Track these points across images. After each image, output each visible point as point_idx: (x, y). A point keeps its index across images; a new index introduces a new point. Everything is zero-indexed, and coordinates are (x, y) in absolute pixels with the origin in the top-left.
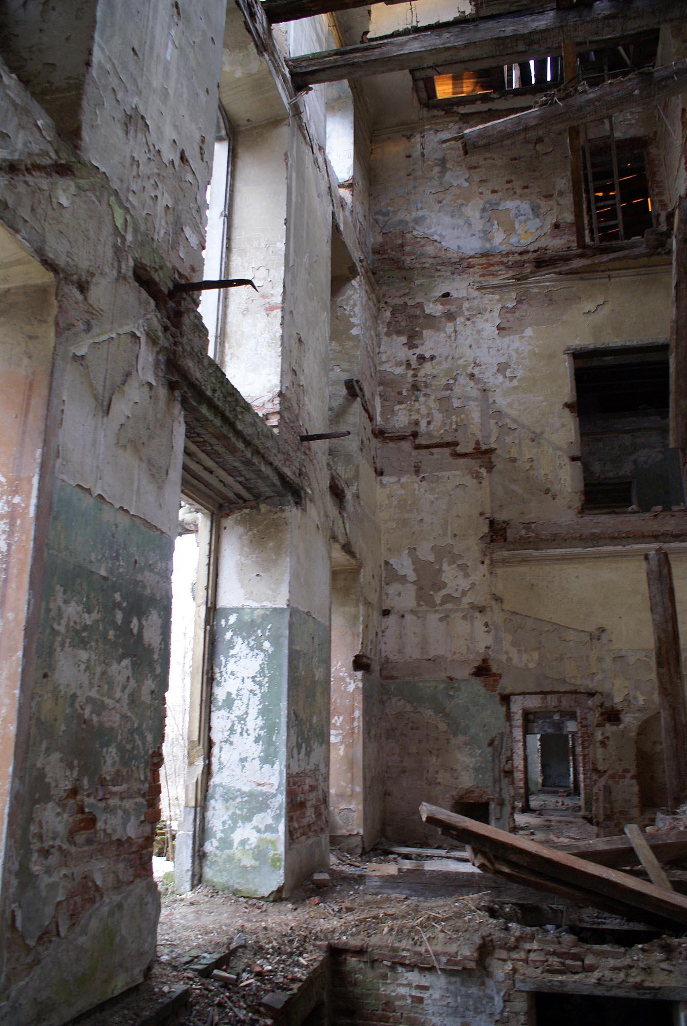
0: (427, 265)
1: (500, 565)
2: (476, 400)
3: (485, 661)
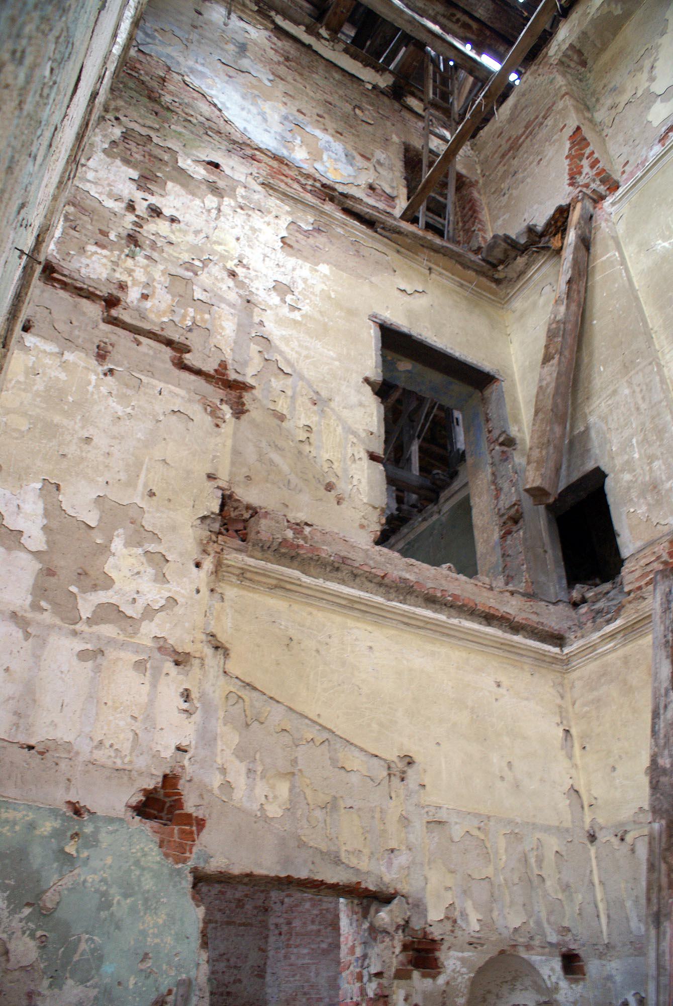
0: (195, 121)
1: (234, 579)
2: (233, 306)
3: (170, 780)
